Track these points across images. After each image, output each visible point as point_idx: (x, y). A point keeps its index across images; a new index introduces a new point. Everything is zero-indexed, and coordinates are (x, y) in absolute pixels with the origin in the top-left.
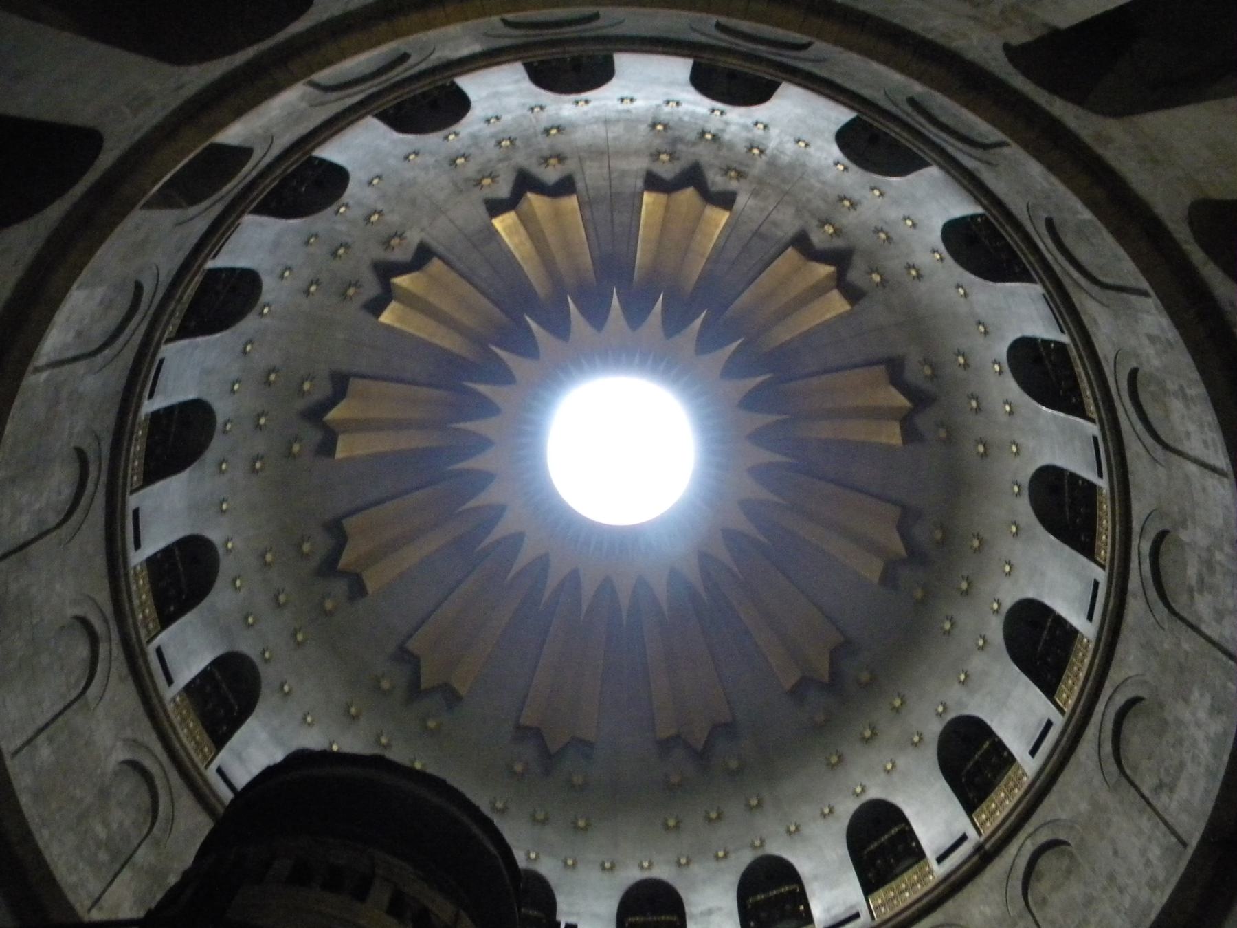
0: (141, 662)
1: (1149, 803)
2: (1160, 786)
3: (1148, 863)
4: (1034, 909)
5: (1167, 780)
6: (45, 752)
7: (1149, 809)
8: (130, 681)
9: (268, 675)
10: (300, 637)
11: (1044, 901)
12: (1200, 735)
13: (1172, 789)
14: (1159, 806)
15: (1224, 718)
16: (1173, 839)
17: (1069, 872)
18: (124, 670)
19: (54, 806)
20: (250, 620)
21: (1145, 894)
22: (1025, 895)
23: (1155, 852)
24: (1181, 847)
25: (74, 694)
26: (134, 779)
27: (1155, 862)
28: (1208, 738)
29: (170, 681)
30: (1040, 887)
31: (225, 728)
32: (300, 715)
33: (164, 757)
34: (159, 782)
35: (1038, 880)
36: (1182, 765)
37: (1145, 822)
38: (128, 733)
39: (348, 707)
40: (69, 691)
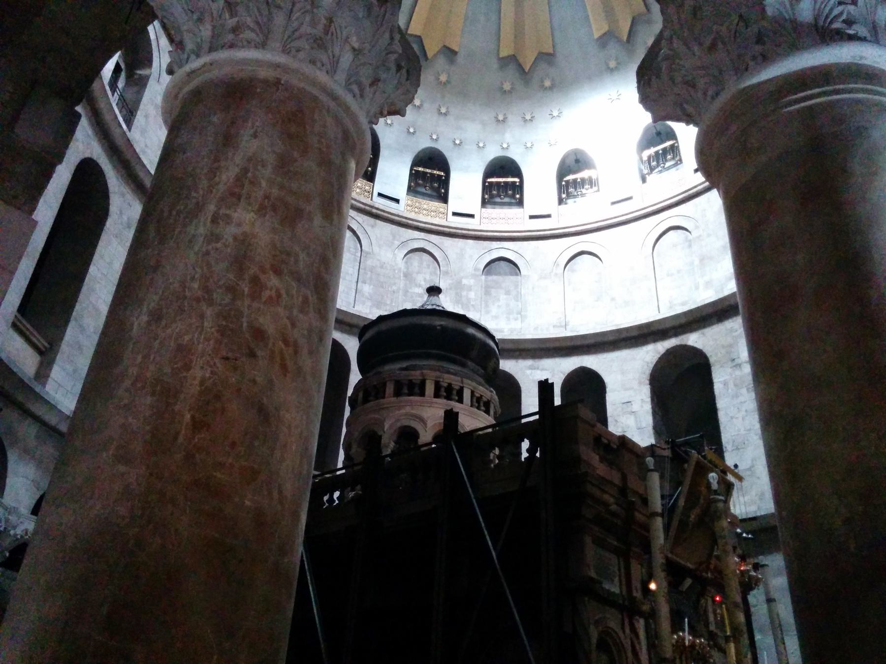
0: (374, 211)
6: (366, 289)
8: (379, 222)
9: (444, 147)
10: (443, 110)
18: (372, 220)
19: (388, 302)
20: (412, 130)
25: (359, 254)
26: (416, 256)
29: (397, 201)
31: (443, 191)
32: (475, 147)
33: (422, 235)
34: (429, 247)
38: (397, 243)
39: (496, 118)
40: (355, 255)
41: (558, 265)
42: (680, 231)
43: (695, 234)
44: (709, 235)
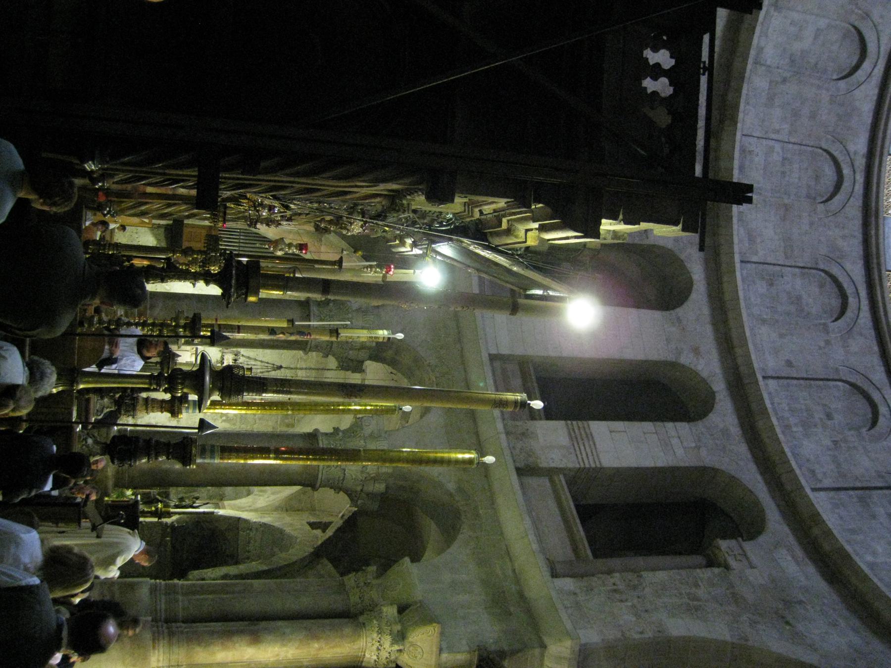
41: (863, 18)
42: (831, 189)
43: (821, 207)
44: (811, 224)
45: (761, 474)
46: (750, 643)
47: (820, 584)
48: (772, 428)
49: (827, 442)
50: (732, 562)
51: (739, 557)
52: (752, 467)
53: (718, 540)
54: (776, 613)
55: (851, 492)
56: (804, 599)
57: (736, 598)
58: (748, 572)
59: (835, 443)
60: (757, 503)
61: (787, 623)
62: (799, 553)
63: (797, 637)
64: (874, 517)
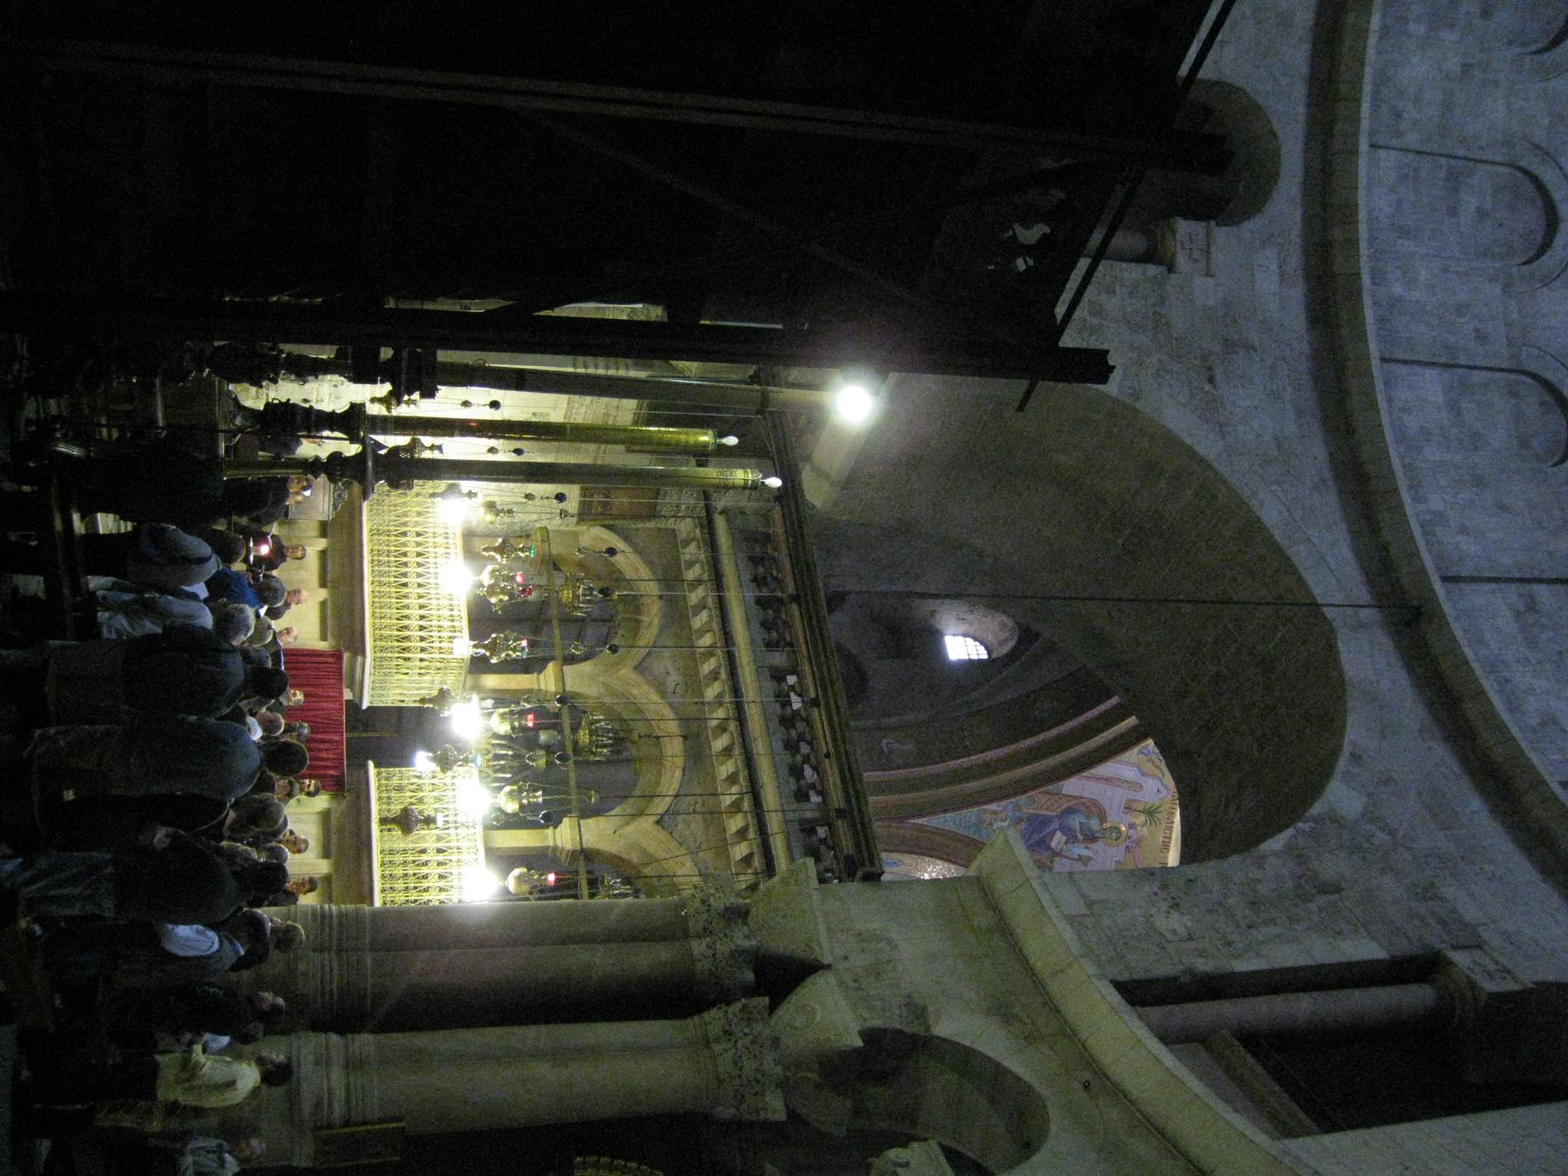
1: (1522, 580)
2: (1531, 606)
3: (1464, 530)
4: (1513, 376)
5: (1531, 619)
7: (1518, 575)
11: (1514, 394)
12: (1540, 684)
13: (1518, 615)
14: (1513, 588)
15: (1534, 722)
16: (1464, 573)
17: (1524, 444)
21: (1435, 502)
22: (1534, 376)
23: (1469, 546)
24: (1452, 572)
27: (1459, 538)
28: (1531, 690)
30: (1533, 398)
35: (1542, 403)
36: (1532, 643)
37: (1506, 562)
45: (1309, 105)
46: (1138, 405)
47: (1296, 321)
48: (1363, 32)
49: (1453, 64)
50: (1182, 261)
51: (1196, 255)
52: (1300, 91)
53: (1179, 218)
54: (1204, 358)
55: (1443, 160)
56: (1257, 344)
57: (1159, 322)
58: (1199, 280)
59: (1466, 67)
60: (1276, 157)
61: (1211, 380)
62: (1295, 259)
63: (1210, 409)
64: (1453, 212)
